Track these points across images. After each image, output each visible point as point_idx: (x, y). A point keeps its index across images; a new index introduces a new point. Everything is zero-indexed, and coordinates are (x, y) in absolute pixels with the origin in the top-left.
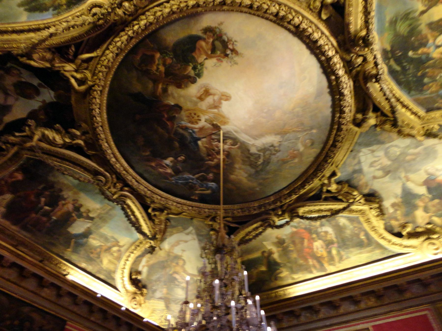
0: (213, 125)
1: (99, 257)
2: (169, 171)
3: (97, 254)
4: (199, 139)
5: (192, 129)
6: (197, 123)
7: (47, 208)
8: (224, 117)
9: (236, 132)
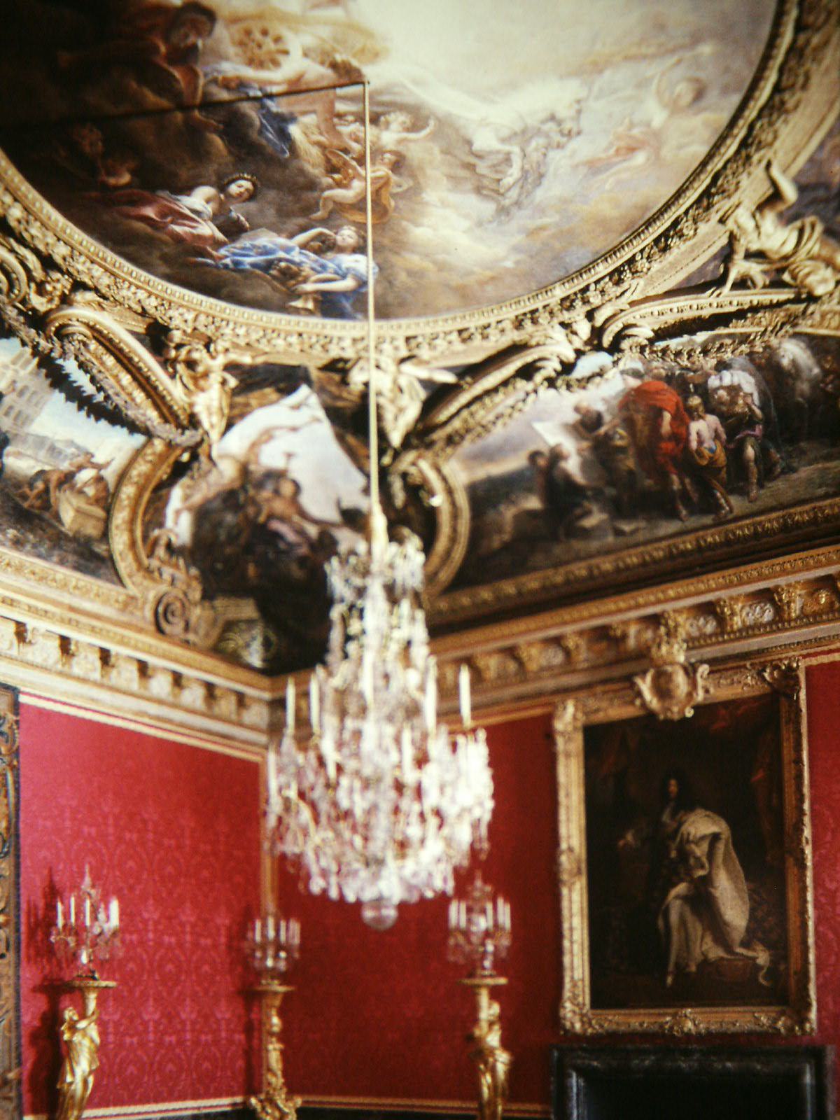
0: (334, 66)
2: (207, 229)
4: (292, 119)
5: (262, 85)
6: (276, 64)
8: (369, 34)
9: (416, 82)
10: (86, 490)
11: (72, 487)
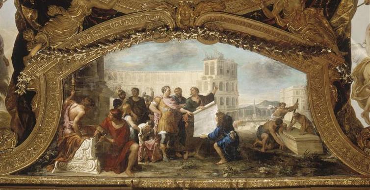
1: (277, 146)
3: (268, 142)
7: (142, 126)
11: (285, 128)
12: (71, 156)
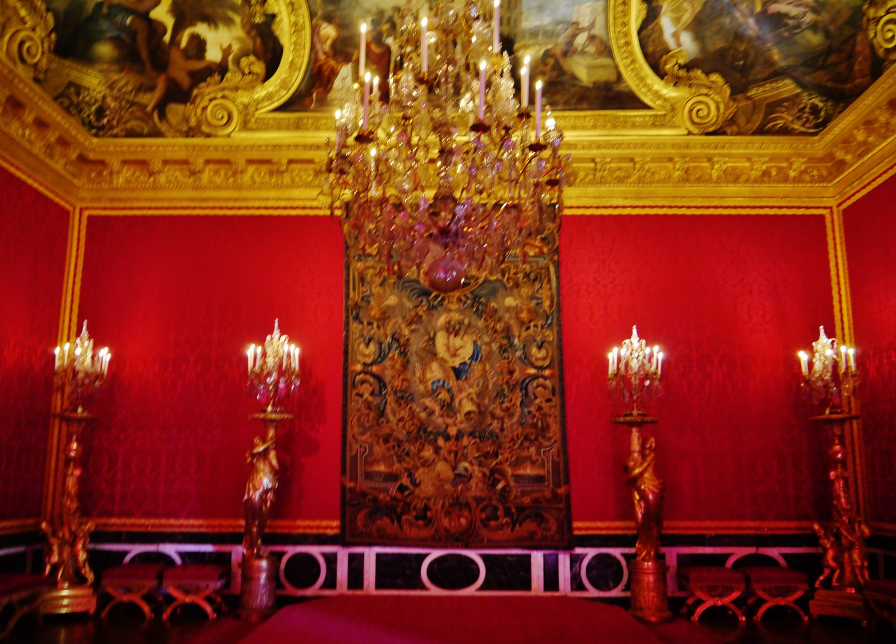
10: (587, 49)
11: (575, 52)
12: (329, 86)
